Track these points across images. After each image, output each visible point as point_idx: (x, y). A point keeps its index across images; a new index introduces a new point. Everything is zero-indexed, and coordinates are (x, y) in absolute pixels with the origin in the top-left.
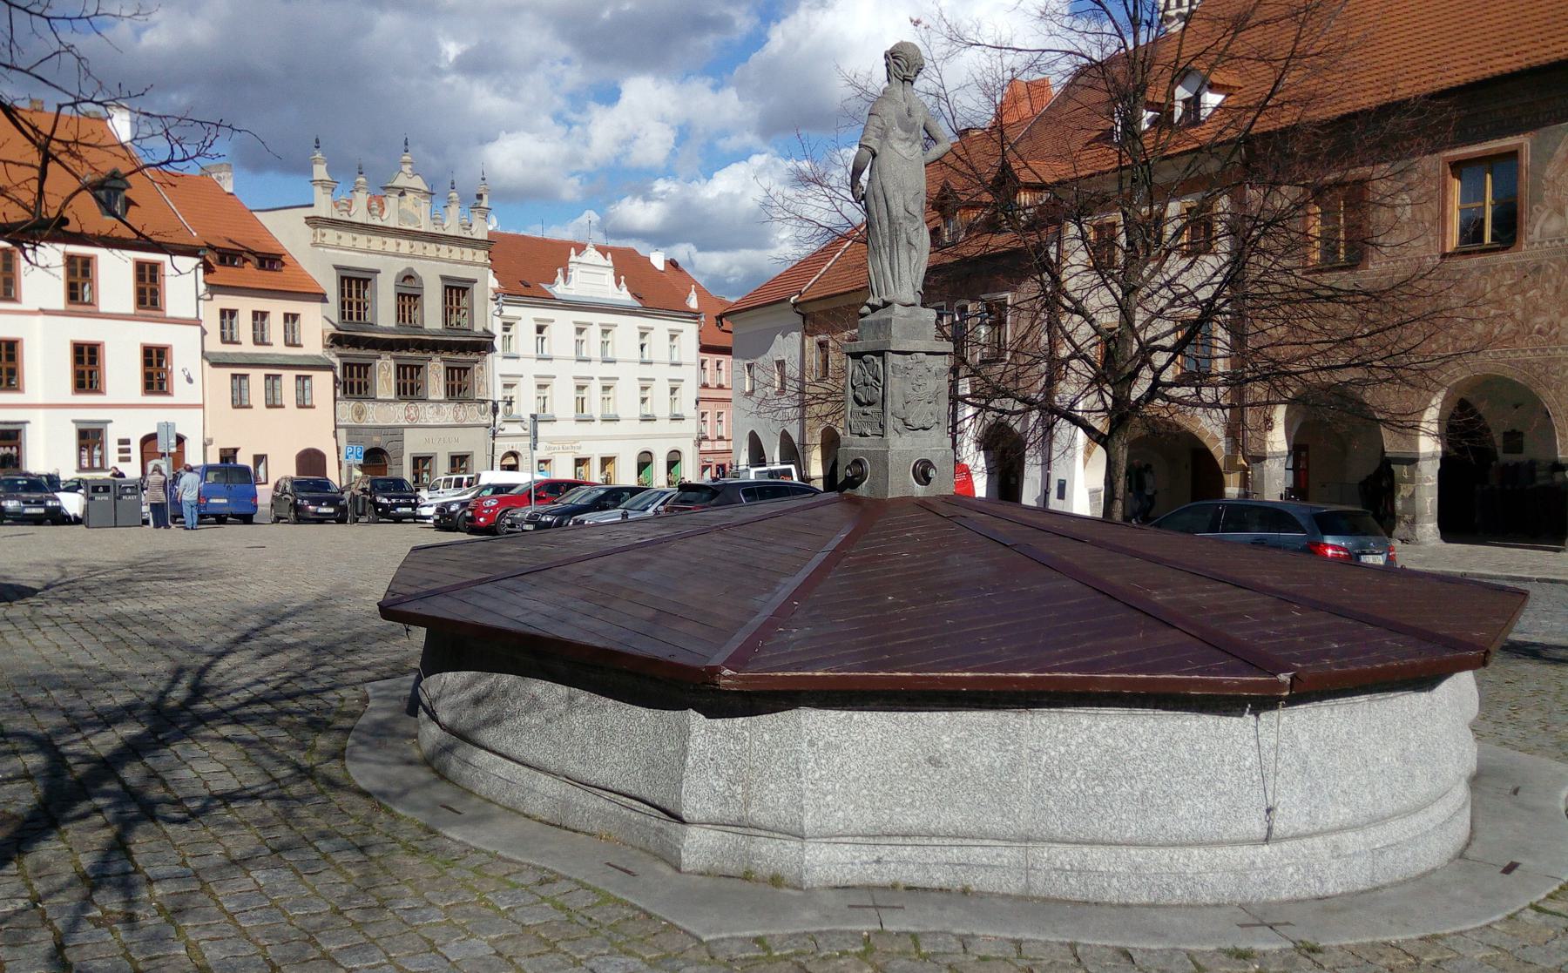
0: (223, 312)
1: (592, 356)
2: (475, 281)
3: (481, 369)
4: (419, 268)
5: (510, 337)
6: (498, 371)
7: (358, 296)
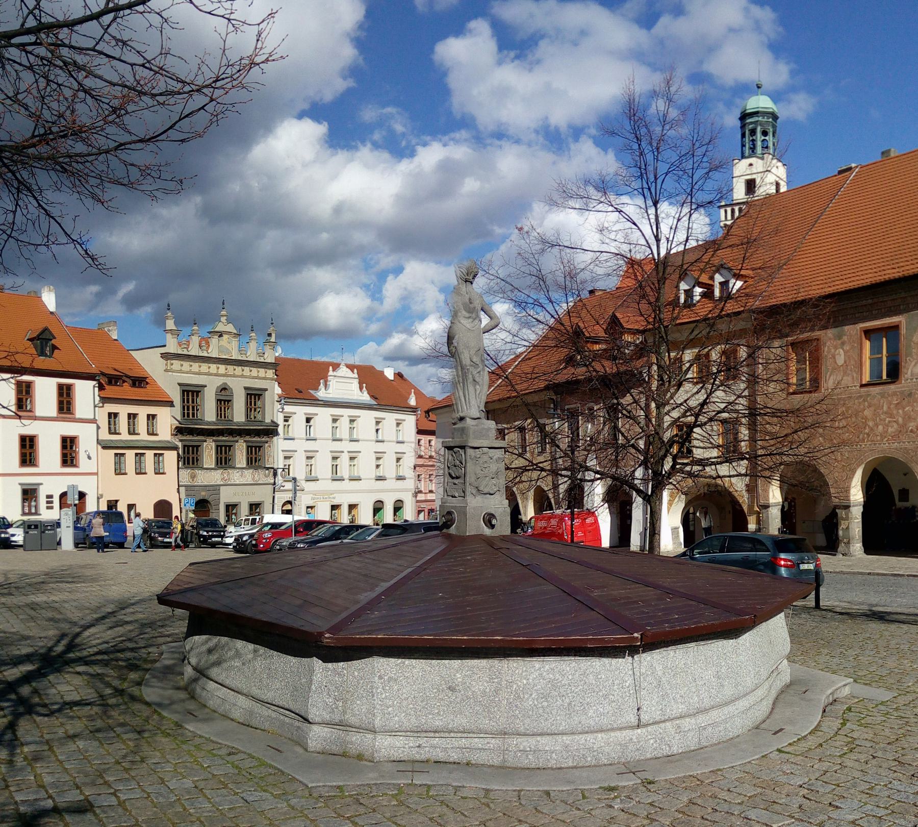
0: (110, 414)
1: (343, 437)
2: (266, 390)
3: (270, 447)
4: (231, 382)
5: (288, 426)
6: (280, 449)
7: (193, 402)
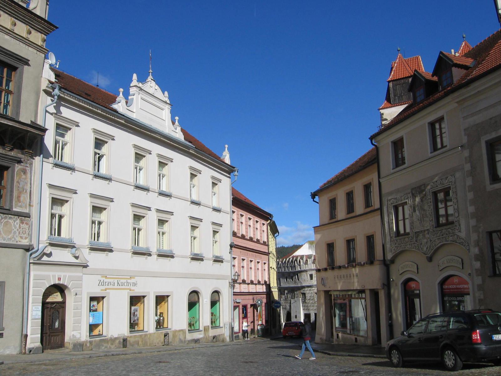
3: (25, 172)
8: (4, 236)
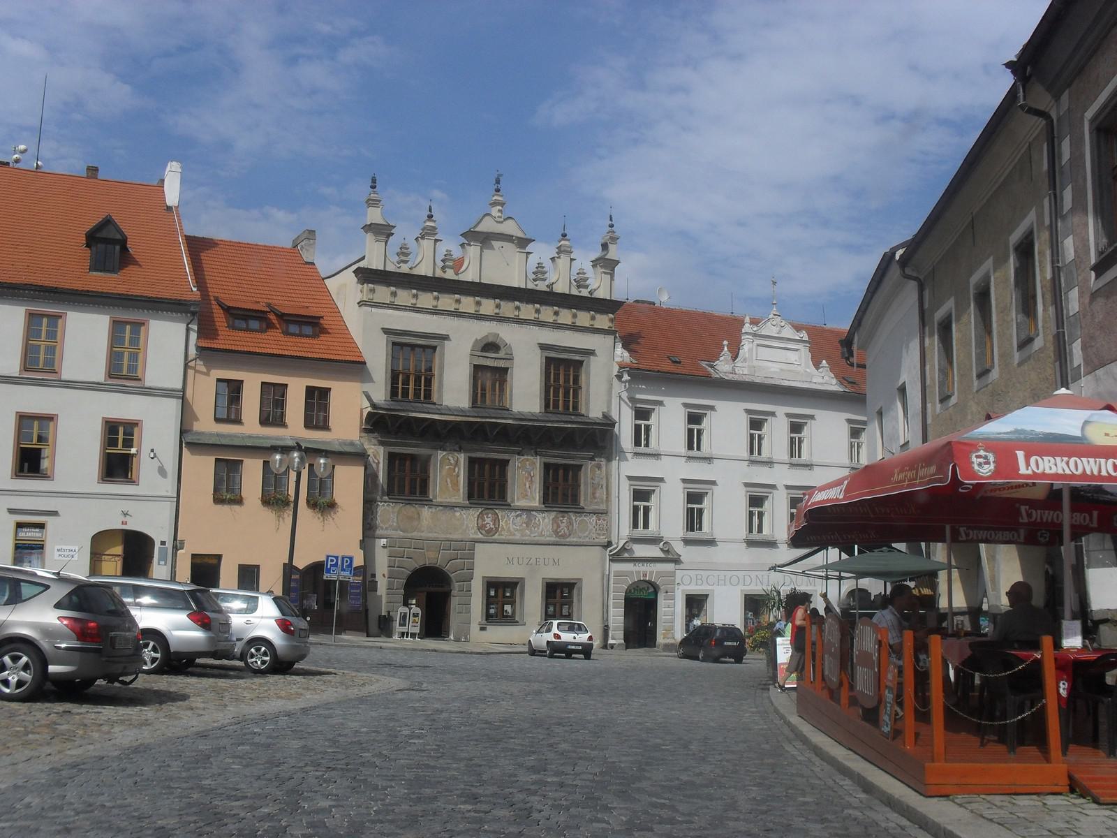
1: (775, 457)
3: (599, 467)
4: (507, 333)
8: (580, 534)
